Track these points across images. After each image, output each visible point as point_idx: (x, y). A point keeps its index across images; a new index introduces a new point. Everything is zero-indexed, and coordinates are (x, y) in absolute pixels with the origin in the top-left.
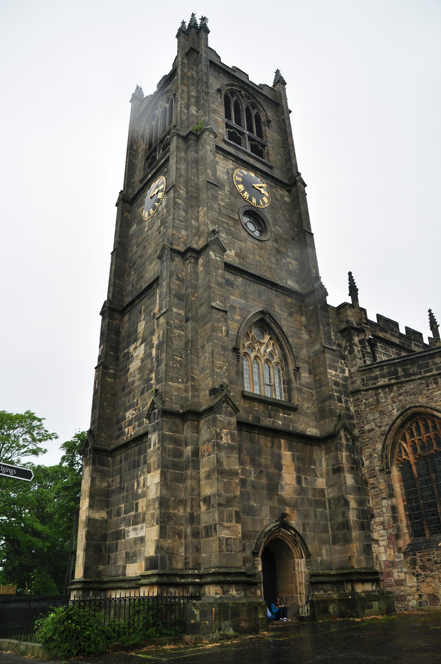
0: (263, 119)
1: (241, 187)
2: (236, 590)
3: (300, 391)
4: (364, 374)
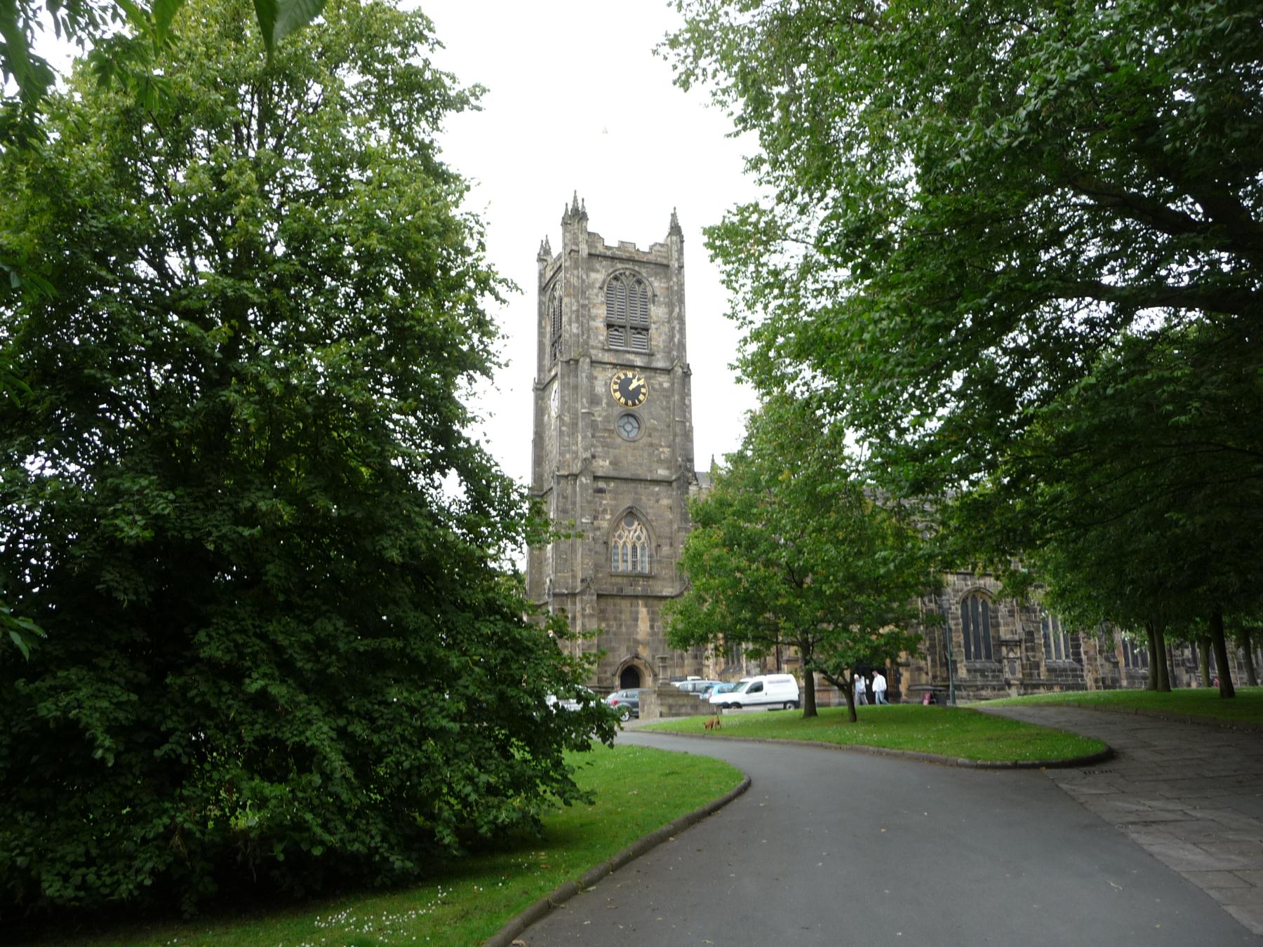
0: (650, 294)
1: (618, 395)
3: (660, 562)
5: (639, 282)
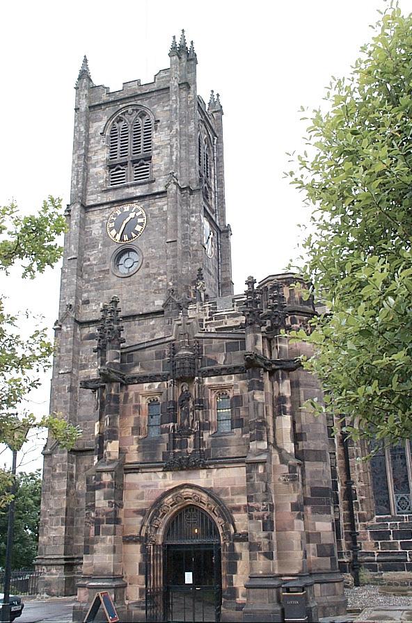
2: (56, 569)
5: (143, 115)
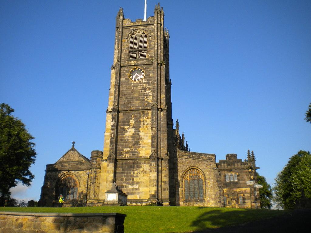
4: (180, 153)
